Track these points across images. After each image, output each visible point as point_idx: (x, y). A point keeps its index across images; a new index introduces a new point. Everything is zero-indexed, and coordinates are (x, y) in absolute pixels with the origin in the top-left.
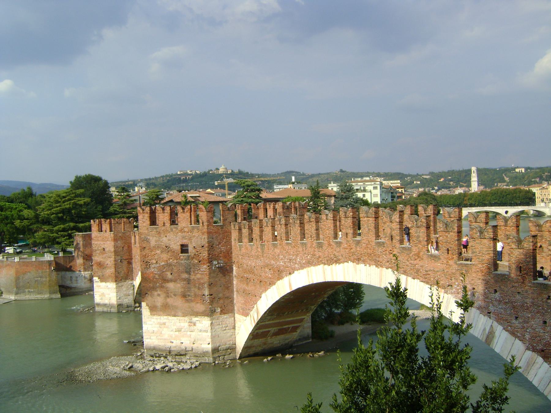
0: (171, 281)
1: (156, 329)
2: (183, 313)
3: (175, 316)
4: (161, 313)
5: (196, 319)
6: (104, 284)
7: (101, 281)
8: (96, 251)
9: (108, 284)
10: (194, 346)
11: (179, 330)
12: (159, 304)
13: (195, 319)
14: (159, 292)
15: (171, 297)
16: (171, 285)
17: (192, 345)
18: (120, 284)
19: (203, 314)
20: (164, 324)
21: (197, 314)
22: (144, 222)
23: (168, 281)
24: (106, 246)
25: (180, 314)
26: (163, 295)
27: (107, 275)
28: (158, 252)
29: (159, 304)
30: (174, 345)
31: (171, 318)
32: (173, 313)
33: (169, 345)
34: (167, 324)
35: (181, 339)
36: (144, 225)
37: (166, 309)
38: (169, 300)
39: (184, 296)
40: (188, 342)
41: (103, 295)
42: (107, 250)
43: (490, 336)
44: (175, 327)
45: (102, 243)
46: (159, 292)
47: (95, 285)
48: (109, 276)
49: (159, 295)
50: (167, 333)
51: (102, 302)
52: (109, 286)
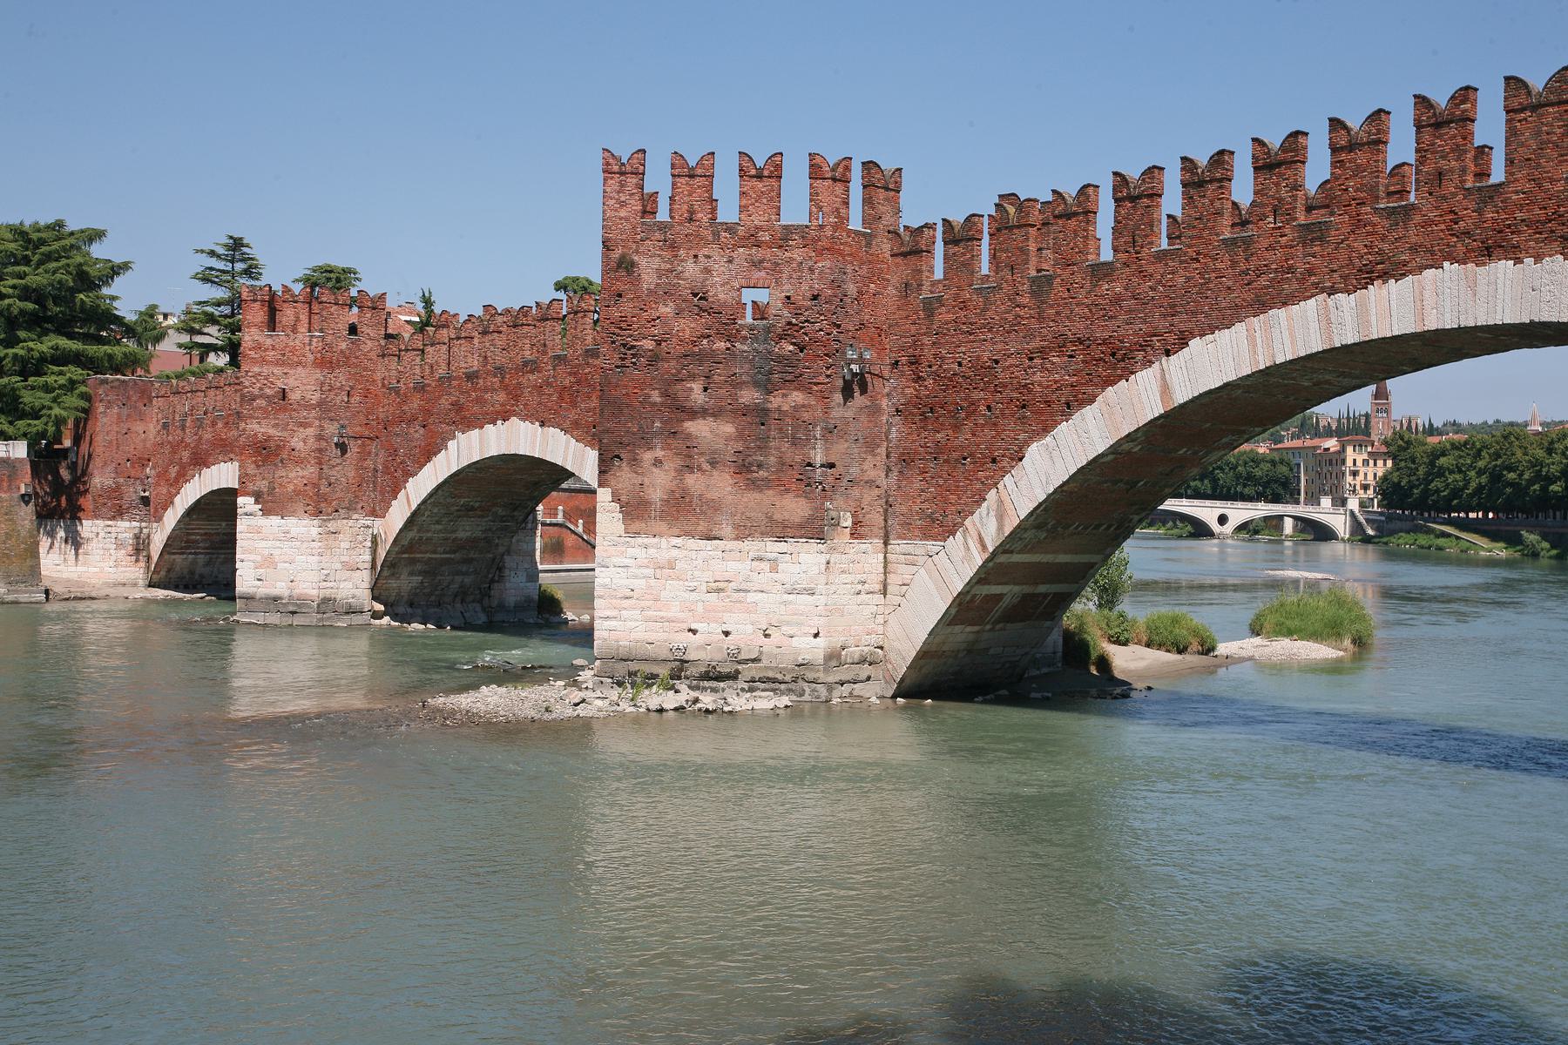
0: (703, 413)
2: (736, 527)
4: (663, 526)
5: (782, 547)
7: (266, 512)
12: (656, 495)
14: (659, 453)
15: (700, 469)
16: (700, 429)
18: (332, 526)
23: (693, 413)
24: (292, 382)
25: (727, 530)
26: (671, 465)
27: (291, 487)
28: (667, 310)
29: (656, 495)
32: (702, 527)
34: (679, 565)
35: (726, 617)
36: (623, 214)
37: (684, 513)
38: (691, 480)
39: (744, 468)
40: (750, 629)
41: (269, 561)
42: (294, 396)
44: (708, 576)
45: (277, 371)
46: (659, 453)
47: (242, 524)
48: (297, 493)
49: (658, 462)
51: (263, 590)
52: (294, 531)
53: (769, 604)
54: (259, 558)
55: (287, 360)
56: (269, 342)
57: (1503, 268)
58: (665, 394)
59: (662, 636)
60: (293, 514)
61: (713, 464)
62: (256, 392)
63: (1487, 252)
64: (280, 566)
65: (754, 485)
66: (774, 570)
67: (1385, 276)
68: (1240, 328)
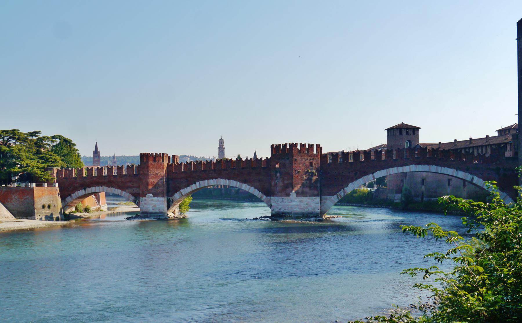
6: (156, 198)
7: (154, 196)
9: (159, 198)
11: (307, 204)
13: (313, 198)
19: (317, 195)
21: (314, 196)
28: (301, 165)
33: (304, 211)
39: (310, 187)
42: (159, 174)
43: (473, 179)
44: (306, 203)
50: (303, 205)
53: (313, 205)
55: (158, 168)
57: (420, 166)
63: (418, 164)
65: (311, 190)
67: (405, 166)
68: (385, 170)
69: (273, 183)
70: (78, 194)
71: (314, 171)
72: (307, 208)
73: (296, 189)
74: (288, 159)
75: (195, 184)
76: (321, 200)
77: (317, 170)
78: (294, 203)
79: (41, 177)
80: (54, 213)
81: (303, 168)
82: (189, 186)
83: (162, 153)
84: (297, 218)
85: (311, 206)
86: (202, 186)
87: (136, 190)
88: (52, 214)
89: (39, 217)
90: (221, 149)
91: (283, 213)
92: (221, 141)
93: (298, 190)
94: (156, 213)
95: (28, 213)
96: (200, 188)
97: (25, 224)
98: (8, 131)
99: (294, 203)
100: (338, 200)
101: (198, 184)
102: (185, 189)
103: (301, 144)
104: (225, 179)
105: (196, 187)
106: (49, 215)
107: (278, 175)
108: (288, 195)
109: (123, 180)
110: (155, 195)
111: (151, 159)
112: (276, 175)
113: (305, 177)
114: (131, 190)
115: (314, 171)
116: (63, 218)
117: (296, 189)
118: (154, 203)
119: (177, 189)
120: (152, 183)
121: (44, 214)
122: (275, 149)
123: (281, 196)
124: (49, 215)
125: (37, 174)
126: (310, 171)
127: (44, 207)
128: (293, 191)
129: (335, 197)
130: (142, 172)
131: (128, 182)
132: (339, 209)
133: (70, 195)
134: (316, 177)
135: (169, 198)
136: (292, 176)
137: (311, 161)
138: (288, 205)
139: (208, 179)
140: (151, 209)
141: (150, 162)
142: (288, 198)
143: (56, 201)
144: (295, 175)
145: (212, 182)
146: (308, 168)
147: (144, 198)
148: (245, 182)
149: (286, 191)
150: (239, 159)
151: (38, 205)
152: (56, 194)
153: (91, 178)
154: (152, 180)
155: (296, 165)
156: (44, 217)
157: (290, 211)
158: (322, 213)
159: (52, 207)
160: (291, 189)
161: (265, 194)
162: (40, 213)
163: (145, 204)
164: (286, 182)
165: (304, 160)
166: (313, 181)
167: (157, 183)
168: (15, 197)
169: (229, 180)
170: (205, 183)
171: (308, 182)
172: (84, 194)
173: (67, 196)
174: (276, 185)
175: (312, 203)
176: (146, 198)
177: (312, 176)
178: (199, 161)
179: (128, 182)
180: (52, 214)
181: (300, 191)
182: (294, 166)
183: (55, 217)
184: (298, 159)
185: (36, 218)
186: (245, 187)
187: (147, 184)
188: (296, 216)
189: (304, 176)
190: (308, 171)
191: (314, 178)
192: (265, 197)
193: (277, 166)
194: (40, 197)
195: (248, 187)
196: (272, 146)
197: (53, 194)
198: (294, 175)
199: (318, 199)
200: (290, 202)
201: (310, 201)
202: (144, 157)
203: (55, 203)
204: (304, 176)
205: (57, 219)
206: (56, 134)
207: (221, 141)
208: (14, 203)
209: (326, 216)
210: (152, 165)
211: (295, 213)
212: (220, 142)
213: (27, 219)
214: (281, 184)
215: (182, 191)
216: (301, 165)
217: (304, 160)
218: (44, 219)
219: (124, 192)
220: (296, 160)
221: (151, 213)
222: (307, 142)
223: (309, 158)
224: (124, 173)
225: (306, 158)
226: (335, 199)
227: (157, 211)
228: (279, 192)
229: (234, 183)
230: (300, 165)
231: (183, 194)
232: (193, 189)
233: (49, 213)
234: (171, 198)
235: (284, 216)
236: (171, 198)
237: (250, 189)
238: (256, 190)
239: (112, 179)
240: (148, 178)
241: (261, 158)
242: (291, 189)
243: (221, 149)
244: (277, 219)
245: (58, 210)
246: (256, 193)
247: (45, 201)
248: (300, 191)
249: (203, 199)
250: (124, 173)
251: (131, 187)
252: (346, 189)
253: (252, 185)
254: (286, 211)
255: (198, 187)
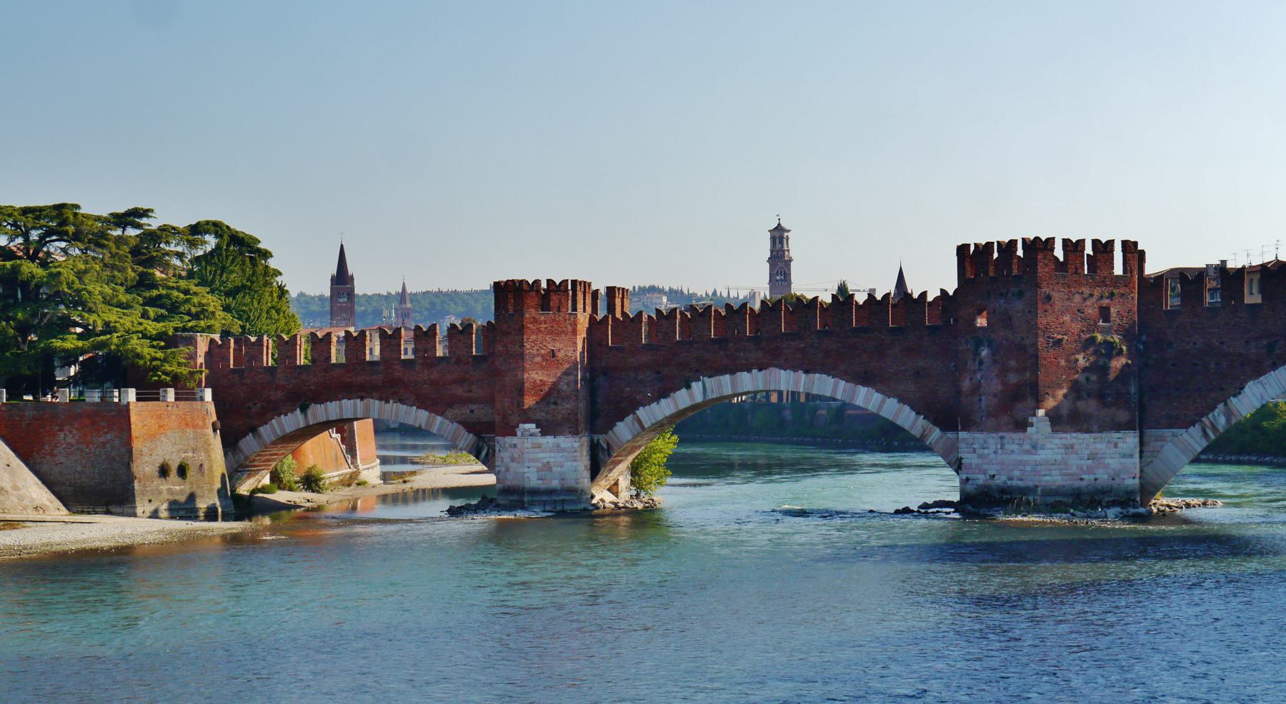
1: (1059, 457)
3: (1088, 431)
6: (549, 440)
7: (544, 433)
8: (534, 356)
10: (1115, 484)
13: (1115, 435)
17: (1111, 482)
20: (1072, 446)
21: (1118, 427)
22: (1046, 265)
24: (558, 345)
25: (1095, 427)
28: (1067, 318)
30: (1084, 484)
31: (1081, 436)
33: (1077, 484)
38: (1081, 405)
39: (1101, 397)
42: (560, 355)
44: (1087, 452)
53: (1114, 463)
54: (540, 465)
55: (556, 333)
56: (542, 318)
58: (1068, 361)
59: (1069, 483)
60: (561, 434)
61: (1089, 395)
62: (535, 352)
64: (555, 469)
65: (1105, 405)
66: (1116, 446)
69: (966, 384)
70: (281, 425)
71: (1116, 338)
72: (1090, 470)
73: (1050, 403)
74: (1020, 294)
75: (688, 387)
76: (1142, 443)
77: (1128, 335)
78: (1042, 455)
79: (156, 369)
80: (198, 492)
81: (1076, 327)
82: (665, 396)
83: (570, 278)
84: (1052, 508)
85: (1107, 466)
86: (710, 396)
87: (480, 412)
88: (192, 497)
89: (150, 508)
90: (779, 262)
91: (1003, 490)
92: (778, 236)
93: (1057, 408)
94: (551, 492)
95: (108, 491)
96: (706, 403)
97: (102, 530)
98: (41, 209)
99: (1042, 455)
100: (1205, 444)
101: (696, 387)
102: (654, 405)
103: (1066, 242)
104: (795, 369)
105: (692, 396)
106: (182, 499)
107: (984, 352)
108: (1021, 425)
109: (435, 375)
110: (547, 428)
111: (532, 300)
112: (976, 353)
113: (1082, 360)
114: (463, 411)
115: (1116, 338)
116: (232, 509)
117: (1050, 403)
118: (544, 456)
119: (625, 408)
120: (537, 386)
121: (166, 496)
122: (972, 259)
123: (996, 429)
124: (182, 499)
125: (139, 356)
126: (1099, 337)
127: (164, 471)
128: (1041, 412)
129: (1195, 431)
130: (500, 348)
131: (454, 382)
132: (1206, 476)
133: (253, 430)
134: (1123, 360)
135: (596, 437)
136: (1037, 357)
137: (1106, 302)
138: (1024, 463)
139: (732, 371)
140: (532, 479)
141: (530, 313)
142: (1021, 435)
143: (207, 452)
144: (1046, 353)
145: (749, 381)
146: (1094, 327)
147: (508, 440)
148: (864, 379)
149: (1012, 411)
150: (843, 297)
151: (144, 466)
152: (204, 427)
153: (326, 370)
154: (536, 376)
155: (1051, 318)
156: (165, 506)
157: (1029, 483)
158: (1148, 490)
159: (191, 473)
160: (1030, 402)
161: (936, 423)
162: (153, 493)
163: (513, 460)
164: (1013, 379)
165: (1077, 298)
166: (1111, 377)
167: (555, 384)
168: (67, 437)
169: (807, 372)
170: (723, 385)
171: (1094, 378)
172: (302, 425)
173: (245, 435)
174: (976, 389)
175: (1111, 455)
176: (515, 440)
177: (1110, 357)
178: (699, 305)
179: (454, 382)
180: (192, 497)
181: (1065, 412)
182: (1042, 321)
183: (202, 505)
184: (1055, 295)
185: (139, 510)
186: (866, 398)
187: (521, 391)
188: (1051, 500)
189: (1080, 357)
190: (1094, 339)
191: (1118, 363)
192: (936, 433)
193: (981, 322)
194: (152, 437)
195: (877, 396)
196: (962, 250)
197: (194, 427)
198: (1042, 354)
199: (1130, 440)
200: (1028, 452)
201: (1101, 447)
202: (509, 294)
203: (202, 456)
204: (1080, 357)
205: (211, 515)
206: (203, 219)
207: (778, 236)
208: (63, 459)
209: (1160, 501)
210: (535, 321)
211: (1048, 492)
212: (773, 239)
213: (108, 512)
214: (996, 386)
215: (641, 412)
216: (1067, 318)
217: (1077, 298)
218: (164, 514)
219: (439, 419)
220: (1049, 298)
221: (534, 492)
222: (1088, 231)
223: (1097, 293)
224: (439, 353)
225: (1086, 291)
226: (1194, 438)
227: (555, 484)
228: (989, 415)
229: (824, 385)
230: (1065, 315)
231: (646, 426)
232: (682, 406)
233: (182, 492)
234: (602, 439)
235: (1008, 502)
236: (602, 439)
237: (883, 402)
238: (907, 408)
239: (398, 372)
240: (523, 370)
241: (924, 294)
242: (1030, 402)
243: (779, 262)
244: (982, 511)
245: (211, 483)
246: (906, 417)
247: (169, 449)
248: (1065, 412)
249: (713, 444)
250: (439, 353)
251: (465, 401)
252: (1233, 400)
253: (888, 393)
254: (1015, 483)
255: (699, 399)
